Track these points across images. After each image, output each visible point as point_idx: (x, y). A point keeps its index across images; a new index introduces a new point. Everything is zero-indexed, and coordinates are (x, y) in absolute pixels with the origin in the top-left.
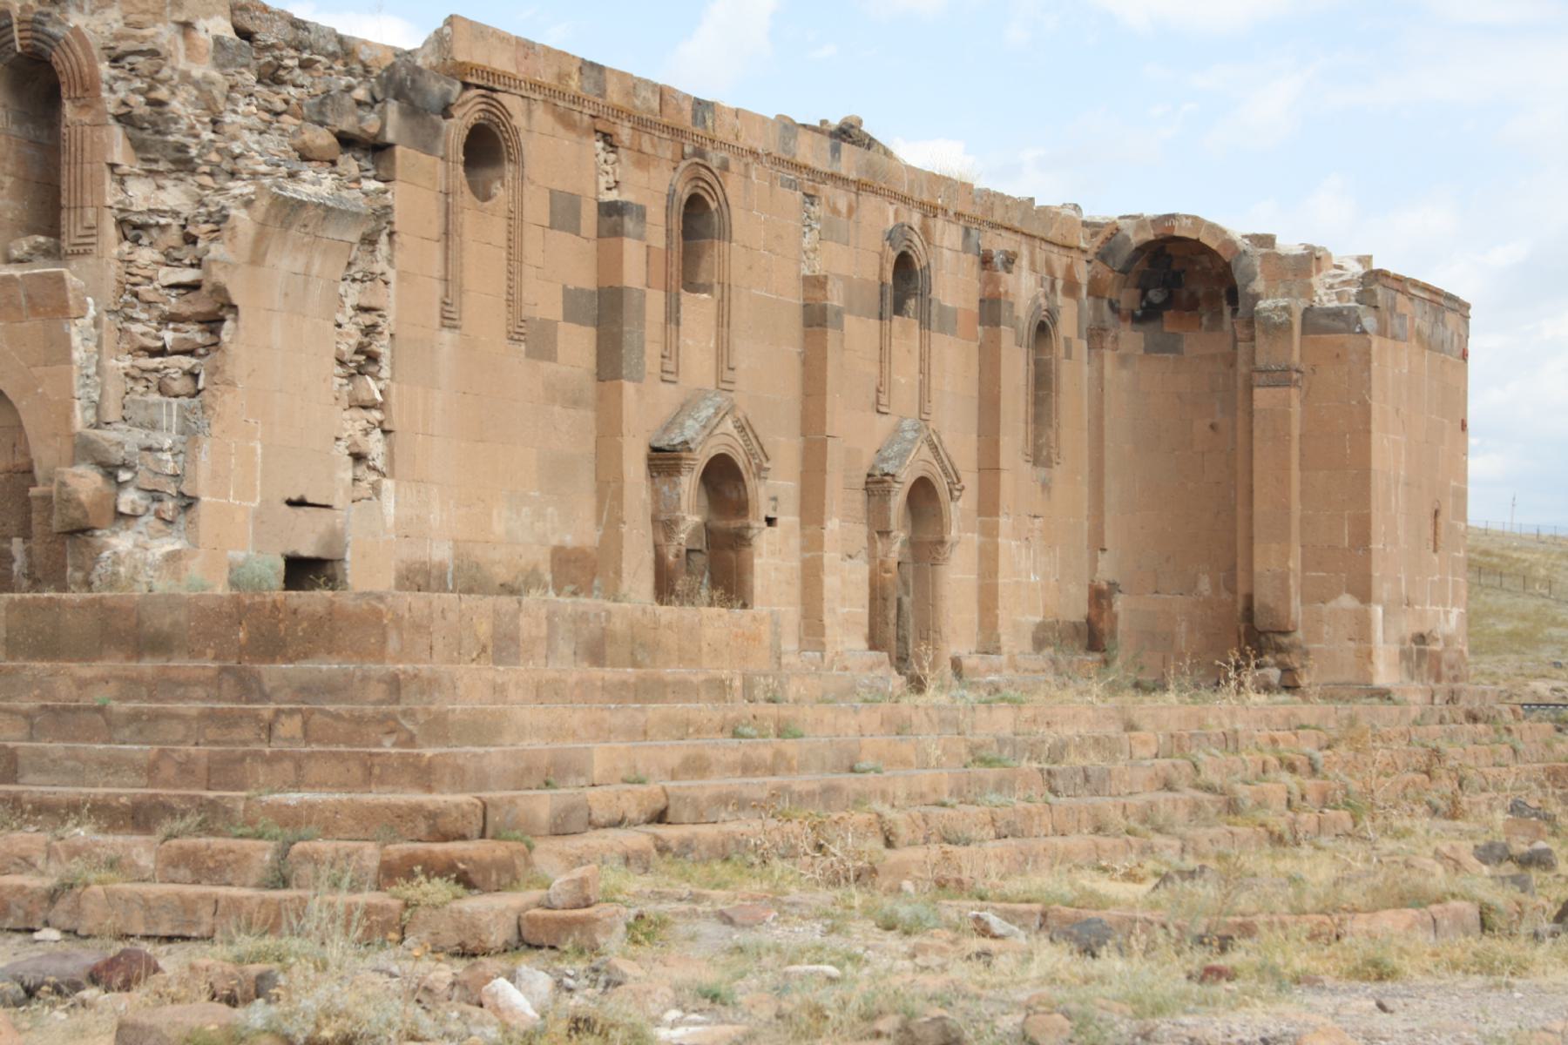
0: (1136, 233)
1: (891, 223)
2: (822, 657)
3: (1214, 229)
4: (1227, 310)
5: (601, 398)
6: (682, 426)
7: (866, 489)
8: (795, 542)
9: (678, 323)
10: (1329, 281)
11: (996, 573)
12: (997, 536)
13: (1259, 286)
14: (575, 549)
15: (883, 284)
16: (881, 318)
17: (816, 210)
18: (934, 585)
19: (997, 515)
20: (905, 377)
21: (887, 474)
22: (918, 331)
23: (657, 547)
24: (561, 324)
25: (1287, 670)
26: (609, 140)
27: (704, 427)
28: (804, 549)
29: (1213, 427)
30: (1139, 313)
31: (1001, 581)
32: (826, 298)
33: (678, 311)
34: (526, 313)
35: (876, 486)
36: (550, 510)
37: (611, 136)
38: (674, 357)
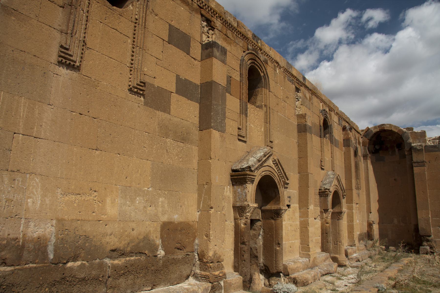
0: (374, 130)
1: (321, 108)
2: (309, 260)
3: (395, 127)
4: (397, 150)
5: (201, 140)
6: (248, 160)
7: (319, 195)
8: (297, 214)
9: (246, 116)
10: (429, 139)
11: (353, 221)
12: (353, 210)
13: (411, 140)
14: (180, 223)
15: (320, 126)
16: (321, 137)
17: (299, 94)
18: (339, 226)
19: (352, 203)
20: (327, 158)
21: (326, 189)
22: (330, 144)
23: (235, 219)
24: (175, 96)
25: (431, 248)
26: (208, 21)
27: (259, 161)
28: (300, 217)
29: (395, 180)
30: (373, 151)
31: (354, 223)
32: (306, 122)
33: (246, 110)
34: (147, 80)
35: (323, 194)
36: (161, 199)
37: (211, 22)
38: (244, 129)
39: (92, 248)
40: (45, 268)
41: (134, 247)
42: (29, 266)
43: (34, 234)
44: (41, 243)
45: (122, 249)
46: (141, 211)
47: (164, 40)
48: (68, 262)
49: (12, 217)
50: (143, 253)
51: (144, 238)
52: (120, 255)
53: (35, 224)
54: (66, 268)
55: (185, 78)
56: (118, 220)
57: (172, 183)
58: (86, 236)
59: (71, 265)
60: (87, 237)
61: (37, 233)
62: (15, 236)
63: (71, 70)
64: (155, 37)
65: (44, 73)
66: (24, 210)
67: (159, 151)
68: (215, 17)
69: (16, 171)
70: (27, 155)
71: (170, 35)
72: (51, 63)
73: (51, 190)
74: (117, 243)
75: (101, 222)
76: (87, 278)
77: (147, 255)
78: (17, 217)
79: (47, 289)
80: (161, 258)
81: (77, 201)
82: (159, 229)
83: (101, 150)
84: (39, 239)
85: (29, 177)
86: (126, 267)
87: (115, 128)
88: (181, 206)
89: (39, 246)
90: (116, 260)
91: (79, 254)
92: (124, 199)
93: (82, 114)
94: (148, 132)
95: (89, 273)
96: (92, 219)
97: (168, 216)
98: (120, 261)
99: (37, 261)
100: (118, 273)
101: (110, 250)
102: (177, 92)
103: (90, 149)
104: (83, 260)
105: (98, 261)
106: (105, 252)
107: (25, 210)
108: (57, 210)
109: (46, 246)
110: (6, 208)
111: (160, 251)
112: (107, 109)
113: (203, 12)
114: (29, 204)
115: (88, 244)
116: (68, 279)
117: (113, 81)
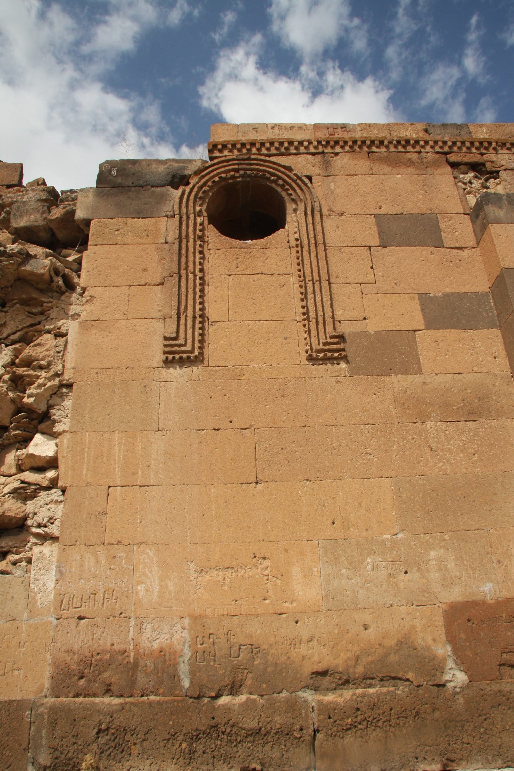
36: (433, 554)
37: (483, 164)
39: (269, 669)
40: (176, 704)
41: (373, 666)
42: (148, 699)
43: (154, 643)
44: (165, 659)
45: (341, 669)
46: (382, 585)
47: (370, 247)
48: (218, 696)
49: (115, 617)
50: (400, 679)
51: (400, 643)
52: (340, 682)
53: (153, 627)
54: (216, 707)
55: (443, 293)
56: (324, 609)
57: (459, 514)
58: (252, 645)
59: (227, 701)
60: (256, 647)
61: (158, 641)
62: (122, 647)
63: (188, 367)
64: (347, 250)
65: (145, 386)
66: (133, 603)
67: (407, 453)
68: (491, 151)
69: (116, 543)
70: (130, 516)
71: (381, 233)
72: (154, 368)
73: (176, 567)
74: (327, 658)
75: (284, 616)
76: (263, 729)
77: (412, 682)
78: (123, 615)
79: (184, 745)
80: (458, 690)
81: (228, 581)
82: (440, 621)
83: (267, 482)
84: (161, 651)
85: (137, 550)
86: (358, 709)
87: (291, 434)
88: (499, 562)
89: (162, 665)
90: (330, 694)
91: (242, 680)
92: (334, 566)
93: (218, 430)
94: (371, 422)
95: (269, 719)
96: (263, 612)
97: (463, 589)
98: (341, 695)
99: (161, 691)
100: (338, 722)
101: (313, 673)
102: (428, 327)
103: (242, 484)
104: (251, 693)
105: (284, 694)
106: (299, 676)
107: (135, 604)
108: (190, 600)
109: (176, 665)
110: (105, 602)
111: (452, 672)
112: (267, 407)
113: (453, 158)
114: (140, 593)
115: (259, 661)
116: (224, 730)
117: (271, 356)
